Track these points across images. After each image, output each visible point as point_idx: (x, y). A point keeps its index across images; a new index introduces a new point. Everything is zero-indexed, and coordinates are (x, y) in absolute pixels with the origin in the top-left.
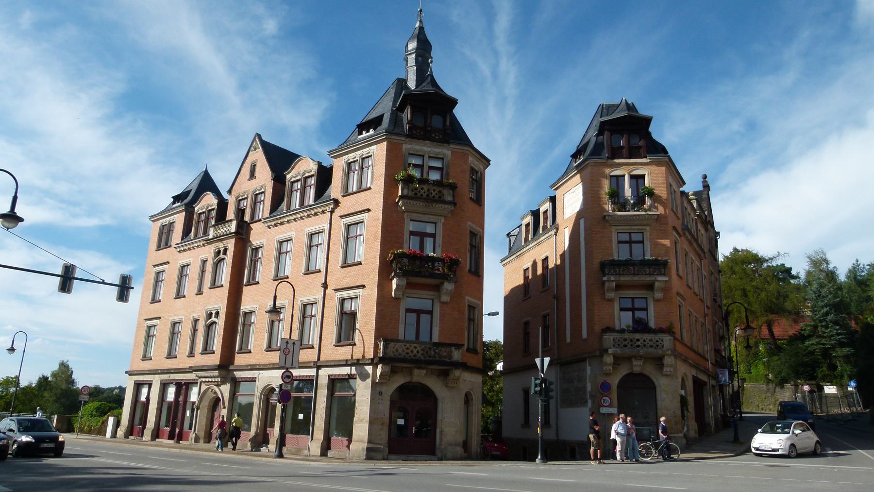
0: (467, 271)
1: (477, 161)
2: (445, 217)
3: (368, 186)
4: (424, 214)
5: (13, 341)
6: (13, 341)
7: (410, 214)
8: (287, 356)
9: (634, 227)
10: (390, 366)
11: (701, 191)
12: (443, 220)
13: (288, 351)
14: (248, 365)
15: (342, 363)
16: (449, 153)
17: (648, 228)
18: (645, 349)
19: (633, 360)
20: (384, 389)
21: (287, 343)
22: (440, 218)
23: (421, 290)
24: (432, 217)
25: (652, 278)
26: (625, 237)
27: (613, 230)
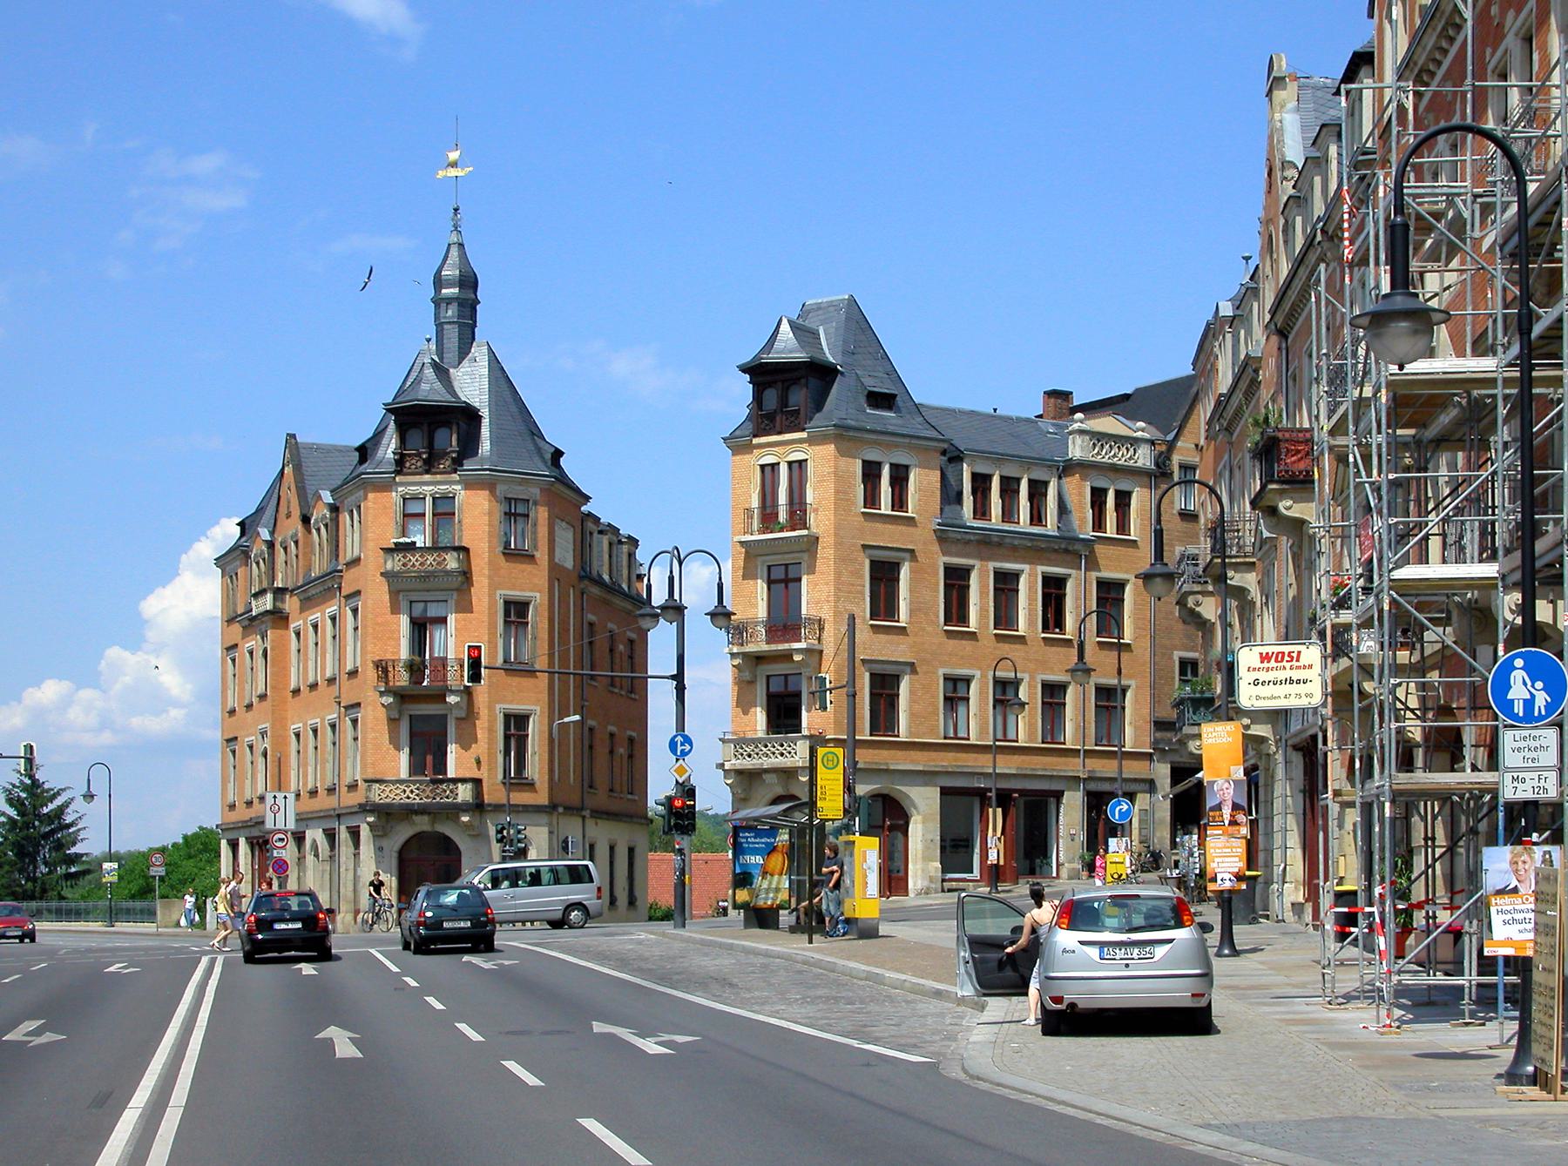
2: (457, 590)
3: (356, 553)
4: (428, 591)
5: (89, 780)
6: (89, 780)
9: (787, 556)
11: (1189, 378)
12: (455, 596)
14: (238, 822)
15: (353, 810)
18: (773, 760)
19: (764, 776)
20: (385, 843)
22: (450, 593)
23: (427, 703)
24: (438, 593)
26: (778, 574)
27: (759, 564)
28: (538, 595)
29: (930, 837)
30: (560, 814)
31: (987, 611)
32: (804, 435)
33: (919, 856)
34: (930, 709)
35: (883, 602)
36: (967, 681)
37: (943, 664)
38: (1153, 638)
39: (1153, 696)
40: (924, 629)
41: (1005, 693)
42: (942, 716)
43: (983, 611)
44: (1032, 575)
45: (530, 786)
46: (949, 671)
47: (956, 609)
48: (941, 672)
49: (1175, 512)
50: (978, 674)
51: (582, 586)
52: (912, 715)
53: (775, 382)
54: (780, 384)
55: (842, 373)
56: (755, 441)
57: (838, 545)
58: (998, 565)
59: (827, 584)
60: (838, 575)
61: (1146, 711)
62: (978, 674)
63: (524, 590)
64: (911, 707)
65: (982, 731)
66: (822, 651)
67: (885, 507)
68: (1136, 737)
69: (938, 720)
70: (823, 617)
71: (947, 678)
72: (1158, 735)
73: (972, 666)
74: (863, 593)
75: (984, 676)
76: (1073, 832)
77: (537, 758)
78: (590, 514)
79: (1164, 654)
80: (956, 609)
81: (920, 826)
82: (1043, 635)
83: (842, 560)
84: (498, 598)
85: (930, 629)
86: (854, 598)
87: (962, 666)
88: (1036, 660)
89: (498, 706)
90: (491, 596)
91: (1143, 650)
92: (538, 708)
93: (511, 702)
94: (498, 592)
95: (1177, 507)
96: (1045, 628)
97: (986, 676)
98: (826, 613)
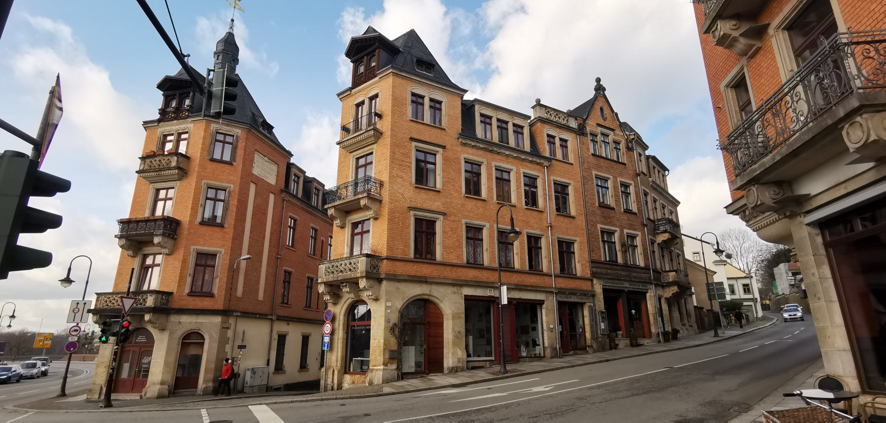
0: (198, 224)
1: (227, 126)
7: (154, 184)
8: (76, 314)
10: (98, 316)
13: (77, 310)
16: (191, 126)
17: (375, 146)
21: (78, 303)
22: (176, 182)
25: (357, 197)
28: (232, 186)
29: (457, 329)
30: (237, 316)
31: (492, 189)
32: (377, 79)
33: (451, 343)
34: (457, 244)
35: (422, 175)
36: (479, 229)
37: (466, 217)
38: (586, 215)
39: (589, 247)
40: (451, 194)
41: (504, 240)
42: (464, 250)
43: (490, 189)
44: (518, 173)
45: (211, 295)
46: (468, 221)
47: (473, 187)
48: (464, 221)
49: (590, 154)
50: (488, 225)
51: (283, 196)
52: (445, 247)
53: (363, 57)
54: (365, 58)
55: (403, 52)
56: (353, 91)
57: (392, 136)
58: (498, 164)
59: (385, 159)
60: (393, 153)
61: (586, 255)
62: (488, 225)
63: (222, 182)
64: (443, 241)
65: (492, 259)
66: (382, 201)
67: (427, 118)
68: (583, 270)
69: (462, 251)
70: (382, 179)
71: (469, 228)
72: (594, 270)
73: (484, 220)
74: (410, 167)
75: (491, 227)
76: (552, 326)
77: (218, 280)
78: (293, 164)
79: (592, 225)
80: (473, 187)
81: (450, 322)
82: (526, 207)
83: (395, 146)
84: (203, 184)
85: (456, 195)
86: (404, 169)
87: (478, 219)
88: (522, 221)
89: (192, 247)
90: (198, 182)
91: (581, 222)
92: (223, 250)
93: (204, 245)
94: (204, 181)
95: (592, 151)
96: (527, 204)
97: (493, 227)
98: (385, 178)
